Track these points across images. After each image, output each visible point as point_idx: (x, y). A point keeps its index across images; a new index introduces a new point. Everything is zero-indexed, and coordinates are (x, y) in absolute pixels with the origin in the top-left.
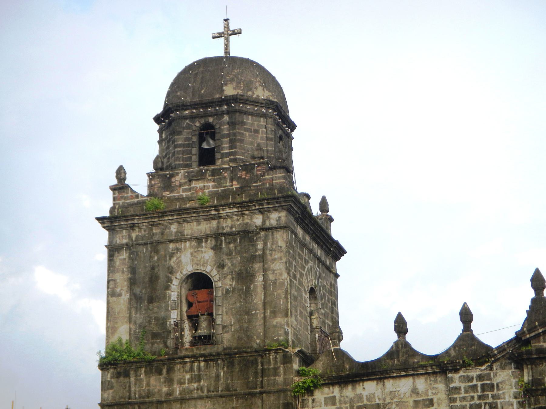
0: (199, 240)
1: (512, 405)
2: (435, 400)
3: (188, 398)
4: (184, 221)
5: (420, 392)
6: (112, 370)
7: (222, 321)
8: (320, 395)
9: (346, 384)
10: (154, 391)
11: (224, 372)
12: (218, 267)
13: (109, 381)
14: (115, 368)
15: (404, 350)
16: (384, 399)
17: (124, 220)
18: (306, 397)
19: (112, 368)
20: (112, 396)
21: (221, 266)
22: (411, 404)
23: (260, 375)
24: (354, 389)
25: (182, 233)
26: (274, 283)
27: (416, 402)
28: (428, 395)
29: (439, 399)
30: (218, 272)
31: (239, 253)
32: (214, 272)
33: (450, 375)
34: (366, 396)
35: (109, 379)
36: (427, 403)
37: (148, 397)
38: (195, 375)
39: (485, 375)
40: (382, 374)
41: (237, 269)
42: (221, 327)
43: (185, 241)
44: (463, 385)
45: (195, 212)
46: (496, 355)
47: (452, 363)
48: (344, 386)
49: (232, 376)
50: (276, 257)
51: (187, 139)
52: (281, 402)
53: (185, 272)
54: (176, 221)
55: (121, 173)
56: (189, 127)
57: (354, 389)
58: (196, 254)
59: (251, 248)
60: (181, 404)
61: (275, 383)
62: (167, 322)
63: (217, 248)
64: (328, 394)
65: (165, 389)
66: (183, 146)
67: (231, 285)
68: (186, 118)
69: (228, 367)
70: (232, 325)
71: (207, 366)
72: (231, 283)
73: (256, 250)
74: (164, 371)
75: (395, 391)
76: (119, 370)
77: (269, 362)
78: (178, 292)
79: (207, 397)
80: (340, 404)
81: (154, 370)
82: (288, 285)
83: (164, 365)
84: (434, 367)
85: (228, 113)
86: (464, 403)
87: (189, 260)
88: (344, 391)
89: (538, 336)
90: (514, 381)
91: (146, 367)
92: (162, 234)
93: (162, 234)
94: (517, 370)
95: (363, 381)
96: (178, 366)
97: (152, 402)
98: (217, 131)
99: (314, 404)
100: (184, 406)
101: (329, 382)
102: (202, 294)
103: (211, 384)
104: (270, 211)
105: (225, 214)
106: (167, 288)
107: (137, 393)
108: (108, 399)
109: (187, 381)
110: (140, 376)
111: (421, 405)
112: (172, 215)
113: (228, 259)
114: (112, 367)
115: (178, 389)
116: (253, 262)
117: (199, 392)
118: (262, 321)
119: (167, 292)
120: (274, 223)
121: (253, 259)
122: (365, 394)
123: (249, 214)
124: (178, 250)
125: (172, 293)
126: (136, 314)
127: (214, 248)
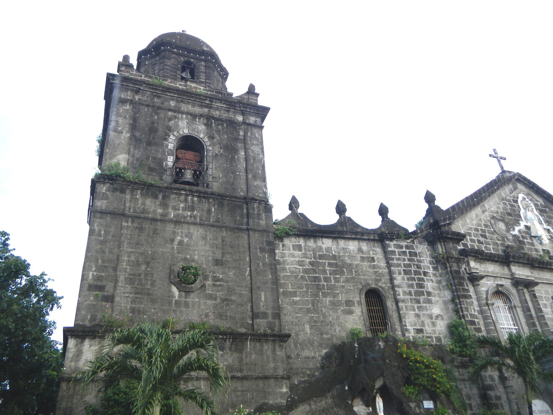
0: (194, 116)
1: (429, 268)
2: (375, 258)
3: (183, 221)
4: (182, 101)
5: (364, 251)
6: (108, 185)
7: (212, 173)
8: (289, 242)
10: (149, 210)
11: (214, 209)
13: (104, 193)
14: (112, 184)
15: (350, 222)
16: (339, 253)
17: (133, 83)
18: (277, 242)
19: (109, 183)
20: (106, 206)
21: (211, 138)
22: (359, 259)
23: (245, 217)
25: (180, 108)
26: (254, 159)
28: (370, 255)
29: (378, 258)
30: (209, 140)
31: (226, 133)
32: (206, 139)
33: (387, 242)
34: (325, 248)
35: (104, 191)
36: (370, 259)
37: (143, 214)
38: (189, 205)
39: (410, 246)
40: (338, 234)
41: (224, 142)
42: (211, 177)
43: (183, 113)
44: (397, 250)
45: (193, 97)
46: (418, 233)
47: (392, 233)
48: (308, 239)
49: (222, 213)
50: (255, 143)
51: (173, 64)
52: (264, 239)
53: (181, 132)
54: (175, 98)
55: (126, 58)
56: (174, 58)
57: (315, 242)
58: (191, 124)
59: (235, 133)
60: (175, 225)
61: (258, 224)
62: (163, 163)
63: (208, 125)
65: (160, 211)
66: (171, 67)
67: (219, 151)
68: (174, 53)
69: (218, 206)
70: (220, 178)
71: (200, 201)
72: (219, 150)
73: (239, 135)
74: (160, 197)
76: (115, 186)
77: (253, 209)
78: (174, 145)
79: (200, 224)
80: (305, 251)
81: (150, 194)
83: (160, 191)
84: (376, 235)
85: (205, 61)
86: (399, 262)
87: (185, 126)
88: (308, 242)
90: (428, 253)
91: (142, 189)
92: (162, 103)
93: (162, 103)
94: (429, 247)
95: (322, 237)
96: (174, 196)
97: (146, 219)
98: (197, 68)
99: (284, 248)
100: (178, 227)
102: (189, 155)
103: (203, 216)
104: (250, 114)
105: (215, 106)
106: (166, 139)
107: (132, 208)
108: (101, 207)
109: (181, 209)
110: (136, 196)
111: (366, 260)
112: (175, 93)
113: (217, 134)
114: (110, 182)
115: (173, 213)
116: (236, 142)
117: (193, 219)
118: (245, 181)
119: (165, 142)
120: (252, 122)
121: (237, 139)
123: (234, 112)
124: (175, 117)
125: (169, 144)
126: (135, 149)
127: (206, 125)
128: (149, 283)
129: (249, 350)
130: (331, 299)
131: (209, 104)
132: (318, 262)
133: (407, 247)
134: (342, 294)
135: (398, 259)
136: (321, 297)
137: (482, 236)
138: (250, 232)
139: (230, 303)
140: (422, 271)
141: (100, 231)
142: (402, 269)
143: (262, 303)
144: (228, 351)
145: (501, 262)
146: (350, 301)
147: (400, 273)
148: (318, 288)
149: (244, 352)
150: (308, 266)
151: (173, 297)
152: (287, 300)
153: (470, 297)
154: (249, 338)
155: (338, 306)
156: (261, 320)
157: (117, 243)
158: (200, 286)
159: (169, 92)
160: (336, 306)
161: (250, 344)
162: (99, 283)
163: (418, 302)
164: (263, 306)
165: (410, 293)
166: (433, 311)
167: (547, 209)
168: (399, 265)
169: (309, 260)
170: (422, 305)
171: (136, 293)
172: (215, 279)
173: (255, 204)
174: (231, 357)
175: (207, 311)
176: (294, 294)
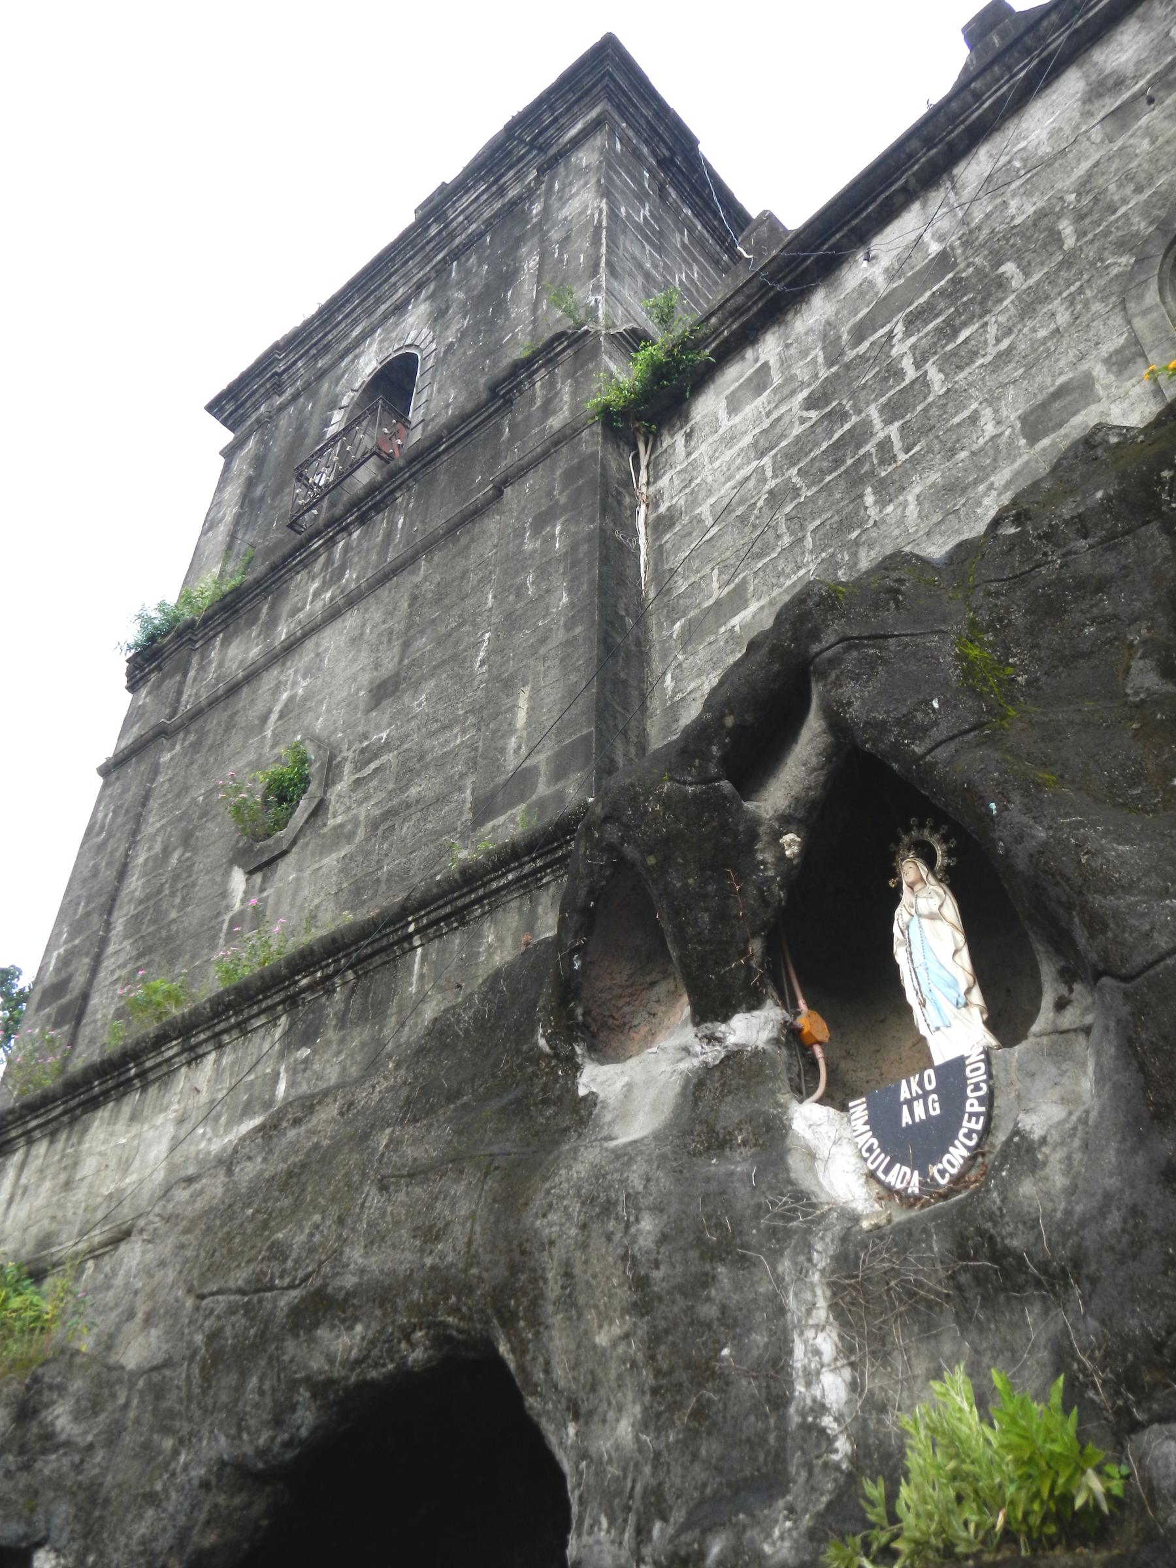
4: (379, 301)
6: (154, 677)
9: (801, 302)
12: (436, 320)
14: (159, 668)
18: (667, 441)
32: (425, 331)
48: (796, 313)
52: (558, 472)
53: (357, 385)
54: (359, 310)
64: (737, 380)
74: (265, 609)
75: (1009, 162)
82: (600, 214)
101: (734, 327)
105: (461, 218)
128: (178, 900)
129: (413, 989)
130: (935, 477)
131: (440, 232)
132: (847, 367)
134: (992, 400)
136: (873, 512)
138: (508, 491)
139: (397, 821)
141: (106, 816)
143: (513, 742)
144: (332, 1034)
146: (1061, 392)
149: (393, 1009)
150: (803, 420)
151: (228, 908)
154: (412, 928)
155: (976, 483)
156: (501, 820)
157: (128, 827)
158: (306, 815)
159: (339, 310)
160: (964, 490)
161: (424, 957)
162: (64, 975)
164: (519, 747)
171: (140, 955)
172: (367, 755)
173: (537, 377)
174: (339, 1053)
175: (317, 901)
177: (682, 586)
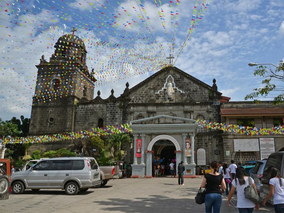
22: (99, 109)
24: (87, 106)
27: (100, 109)
55: (43, 57)
89: (125, 96)
122: (89, 107)
133: (113, 104)
135: (109, 109)
137: (141, 96)
140: (116, 112)
142: (109, 112)
145: (144, 106)
147: (109, 113)
148: (86, 119)
152: (77, 123)
153: (127, 119)
163: (112, 121)
165: (110, 119)
166: (116, 124)
167: (180, 79)
168: (109, 111)
169: (84, 112)
170: (113, 122)
176: (79, 121)
177: (77, 118)
